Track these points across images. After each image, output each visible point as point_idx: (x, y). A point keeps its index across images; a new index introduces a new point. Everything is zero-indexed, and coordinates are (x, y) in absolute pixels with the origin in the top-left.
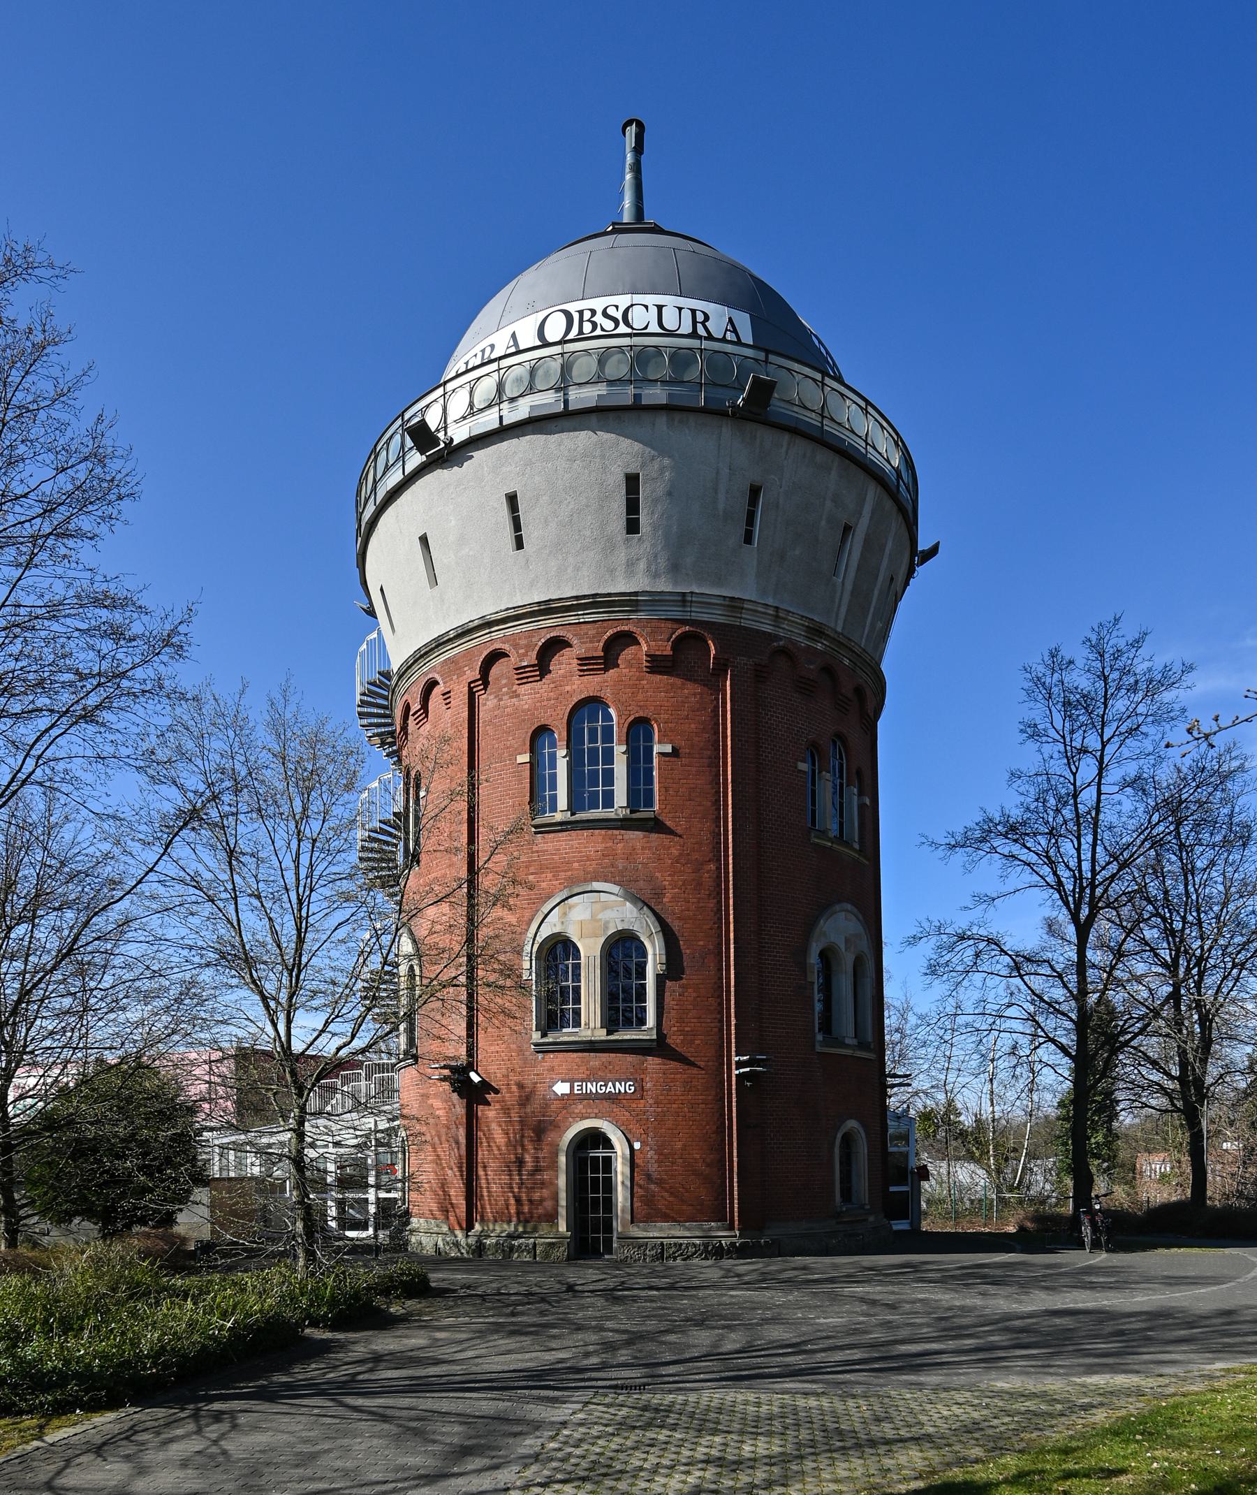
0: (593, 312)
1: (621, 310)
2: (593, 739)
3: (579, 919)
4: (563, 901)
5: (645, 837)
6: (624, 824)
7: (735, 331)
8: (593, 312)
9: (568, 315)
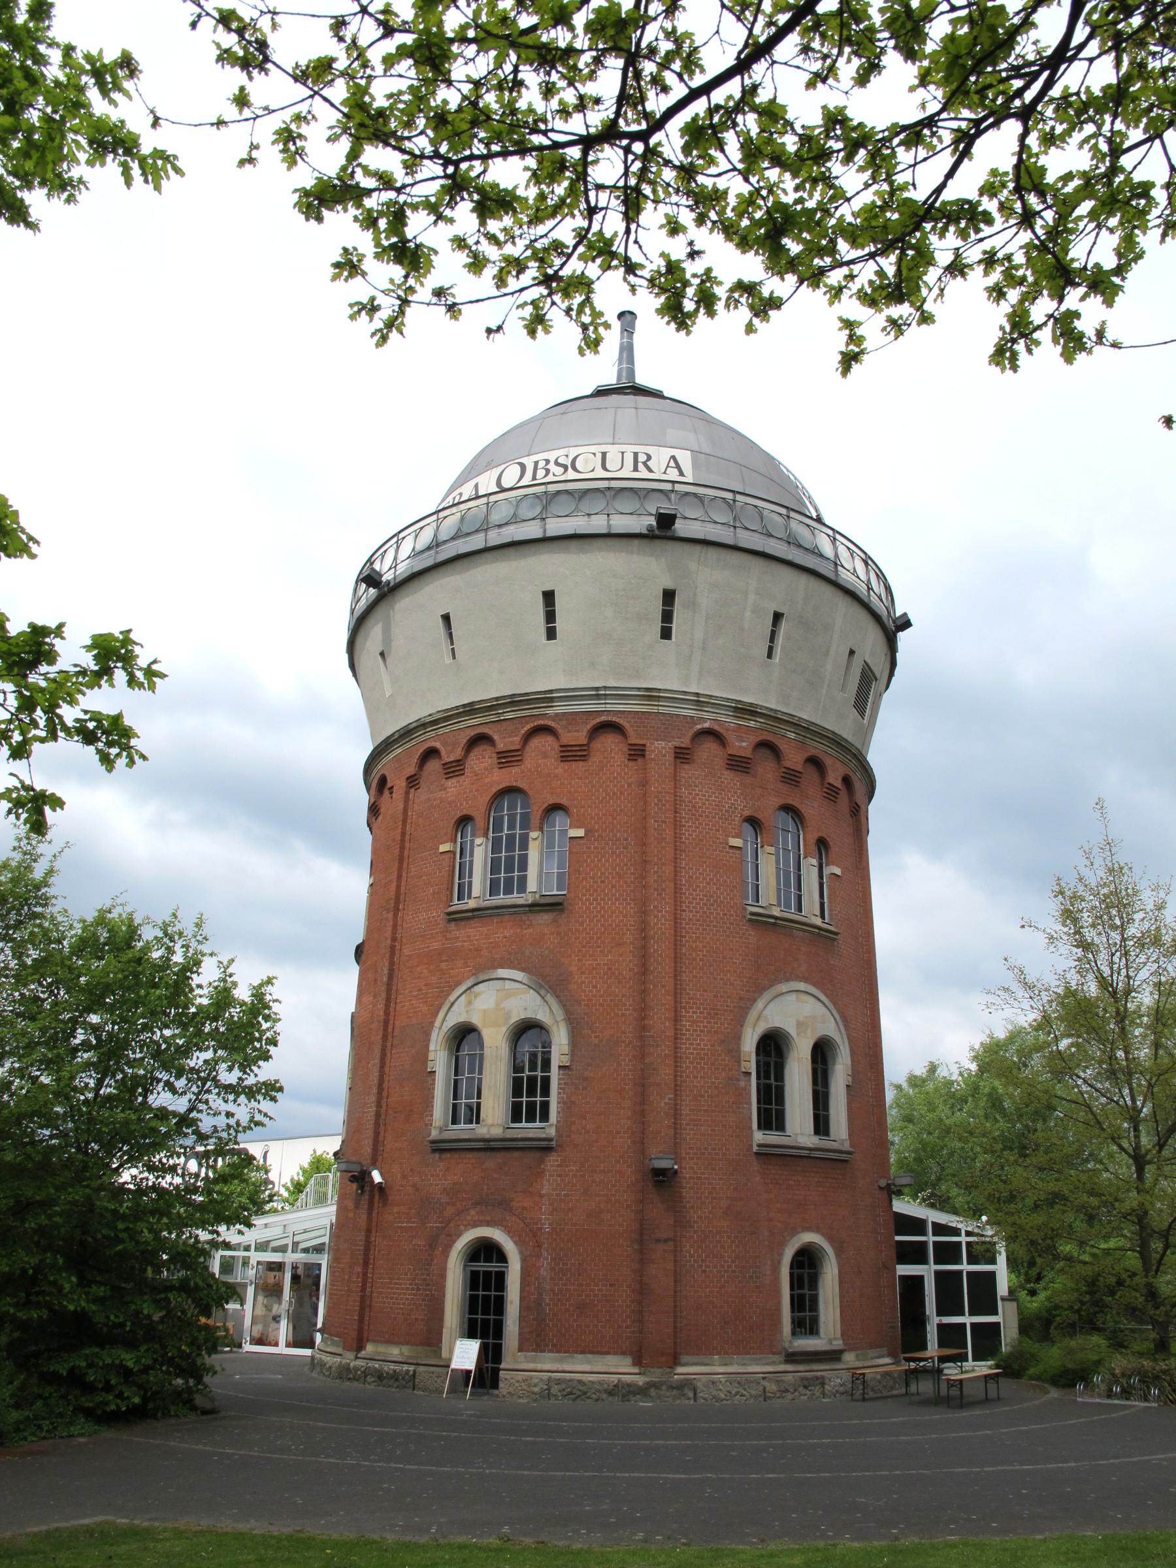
0: (548, 462)
1: (571, 458)
2: (512, 826)
3: (485, 1007)
4: (469, 988)
5: (554, 921)
6: (536, 907)
7: (678, 467)
8: (548, 462)
9: (523, 467)
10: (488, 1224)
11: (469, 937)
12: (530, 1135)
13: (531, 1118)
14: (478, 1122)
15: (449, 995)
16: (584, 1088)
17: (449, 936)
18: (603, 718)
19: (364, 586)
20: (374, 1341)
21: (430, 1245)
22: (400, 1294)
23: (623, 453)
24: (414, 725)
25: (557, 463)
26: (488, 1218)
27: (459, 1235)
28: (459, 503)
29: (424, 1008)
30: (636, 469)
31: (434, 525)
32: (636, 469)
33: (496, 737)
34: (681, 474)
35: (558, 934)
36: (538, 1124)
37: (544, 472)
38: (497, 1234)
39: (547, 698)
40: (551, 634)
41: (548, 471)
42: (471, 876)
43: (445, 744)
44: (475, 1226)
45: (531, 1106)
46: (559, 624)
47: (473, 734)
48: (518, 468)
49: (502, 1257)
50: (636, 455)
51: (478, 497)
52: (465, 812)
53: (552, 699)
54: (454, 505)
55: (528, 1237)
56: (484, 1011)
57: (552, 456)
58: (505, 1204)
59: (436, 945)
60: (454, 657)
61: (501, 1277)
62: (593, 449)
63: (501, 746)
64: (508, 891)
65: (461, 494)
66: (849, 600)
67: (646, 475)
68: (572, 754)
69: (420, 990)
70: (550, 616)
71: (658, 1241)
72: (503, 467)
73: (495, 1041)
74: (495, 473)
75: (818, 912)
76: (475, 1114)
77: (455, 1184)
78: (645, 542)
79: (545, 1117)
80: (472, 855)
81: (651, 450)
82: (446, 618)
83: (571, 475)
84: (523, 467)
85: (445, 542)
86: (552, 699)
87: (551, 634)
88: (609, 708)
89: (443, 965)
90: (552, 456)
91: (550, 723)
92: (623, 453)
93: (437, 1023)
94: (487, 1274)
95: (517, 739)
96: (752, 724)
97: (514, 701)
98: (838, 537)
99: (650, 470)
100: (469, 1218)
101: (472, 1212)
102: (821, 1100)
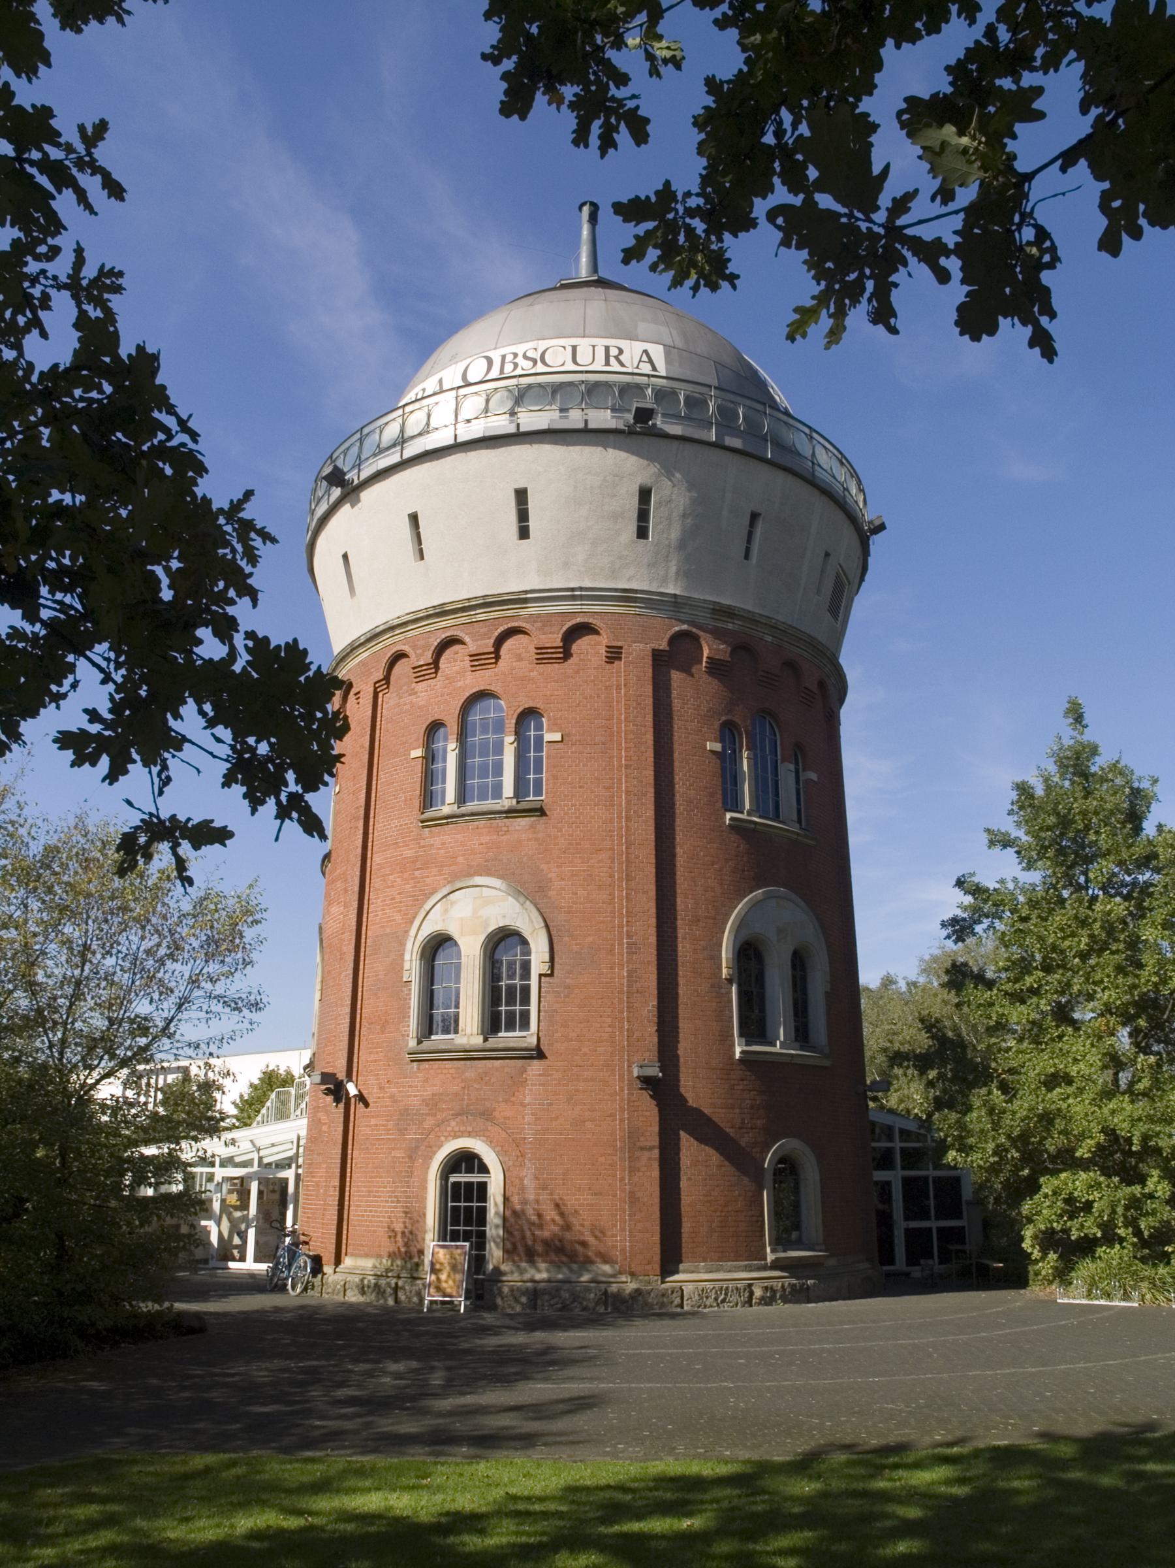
0: (515, 355)
1: (540, 352)
4: (445, 897)
5: (532, 826)
6: (510, 813)
7: (651, 361)
8: (515, 355)
9: (490, 361)
10: (470, 1135)
11: (444, 844)
12: (511, 1045)
13: (510, 1027)
14: (456, 1032)
15: (425, 902)
16: (565, 997)
17: (422, 843)
18: (579, 620)
19: (325, 483)
20: (353, 1255)
21: (410, 1157)
22: (379, 1207)
23: (594, 347)
24: (382, 628)
25: (525, 357)
26: (470, 1129)
27: (440, 1147)
28: (423, 398)
29: (398, 917)
30: (607, 363)
31: (400, 420)
32: (607, 363)
33: (467, 639)
34: (654, 369)
35: (536, 839)
36: (517, 1034)
37: (511, 366)
38: (478, 1146)
39: (520, 600)
40: (524, 533)
41: (516, 365)
42: (444, 782)
43: (414, 647)
44: (456, 1137)
45: (511, 1016)
46: (533, 523)
47: (443, 636)
48: (485, 362)
49: (484, 1169)
50: (607, 349)
51: (442, 391)
52: (437, 717)
53: (526, 601)
54: (417, 400)
55: (510, 1148)
56: (462, 919)
57: (520, 349)
58: (487, 1115)
59: (409, 853)
60: (422, 558)
61: (483, 1187)
62: (562, 342)
63: (472, 647)
64: (483, 796)
65: (424, 390)
66: (825, 499)
67: (618, 368)
68: (543, 655)
69: (393, 899)
70: (523, 515)
71: (643, 1149)
72: (468, 361)
73: (471, 949)
74: (461, 367)
75: (795, 817)
76: (451, 1025)
77: (434, 1095)
78: (621, 437)
79: (525, 1025)
80: (445, 760)
81: (624, 344)
82: (414, 518)
83: (541, 368)
84: (490, 361)
85: (413, 437)
86: (526, 601)
87: (524, 533)
88: (585, 609)
89: (417, 873)
90: (520, 349)
91: (524, 625)
92: (594, 347)
93: (412, 933)
94: (469, 1185)
95: (492, 641)
96: (730, 626)
97: (487, 603)
98: (815, 435)
99: (622, 365)
100: (449, 1129)
101: (453, 1123)
102: (800, 1009)
